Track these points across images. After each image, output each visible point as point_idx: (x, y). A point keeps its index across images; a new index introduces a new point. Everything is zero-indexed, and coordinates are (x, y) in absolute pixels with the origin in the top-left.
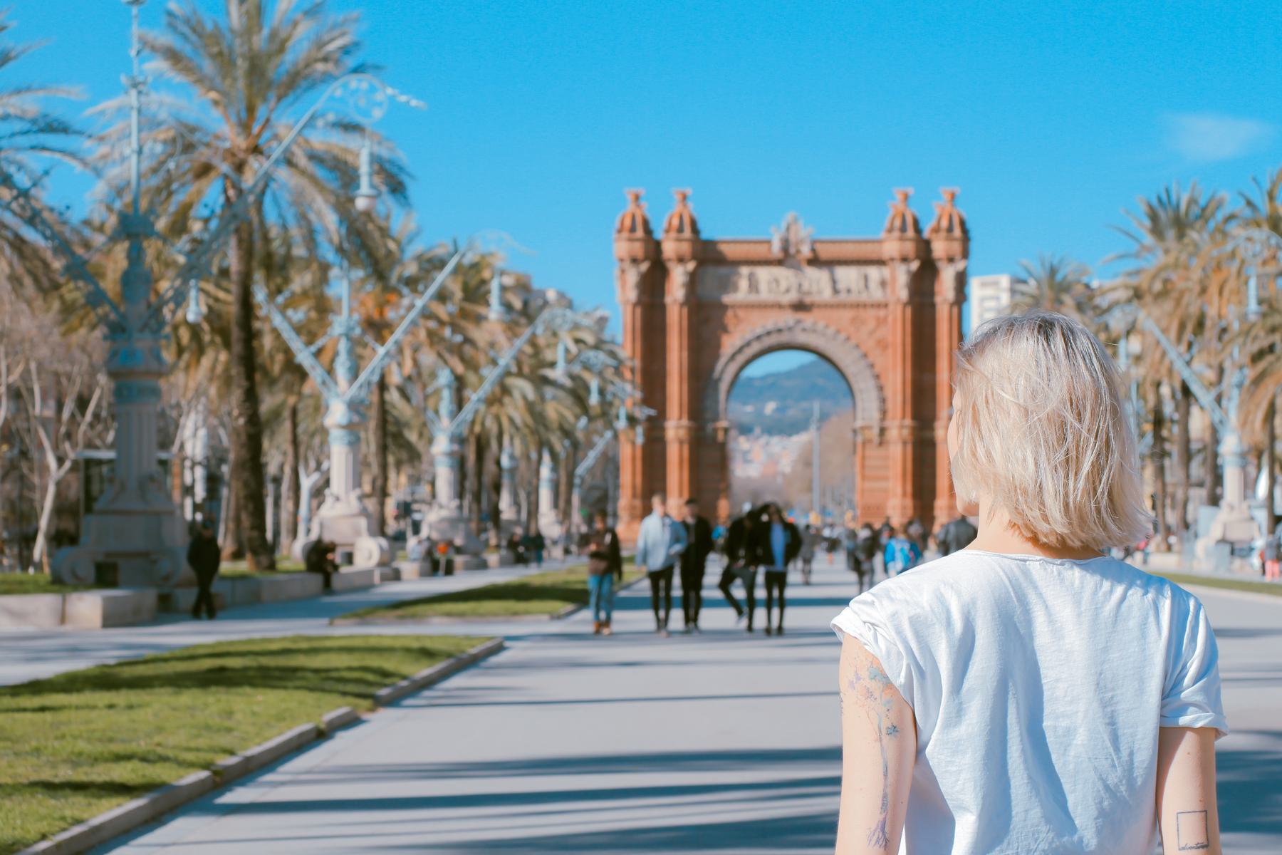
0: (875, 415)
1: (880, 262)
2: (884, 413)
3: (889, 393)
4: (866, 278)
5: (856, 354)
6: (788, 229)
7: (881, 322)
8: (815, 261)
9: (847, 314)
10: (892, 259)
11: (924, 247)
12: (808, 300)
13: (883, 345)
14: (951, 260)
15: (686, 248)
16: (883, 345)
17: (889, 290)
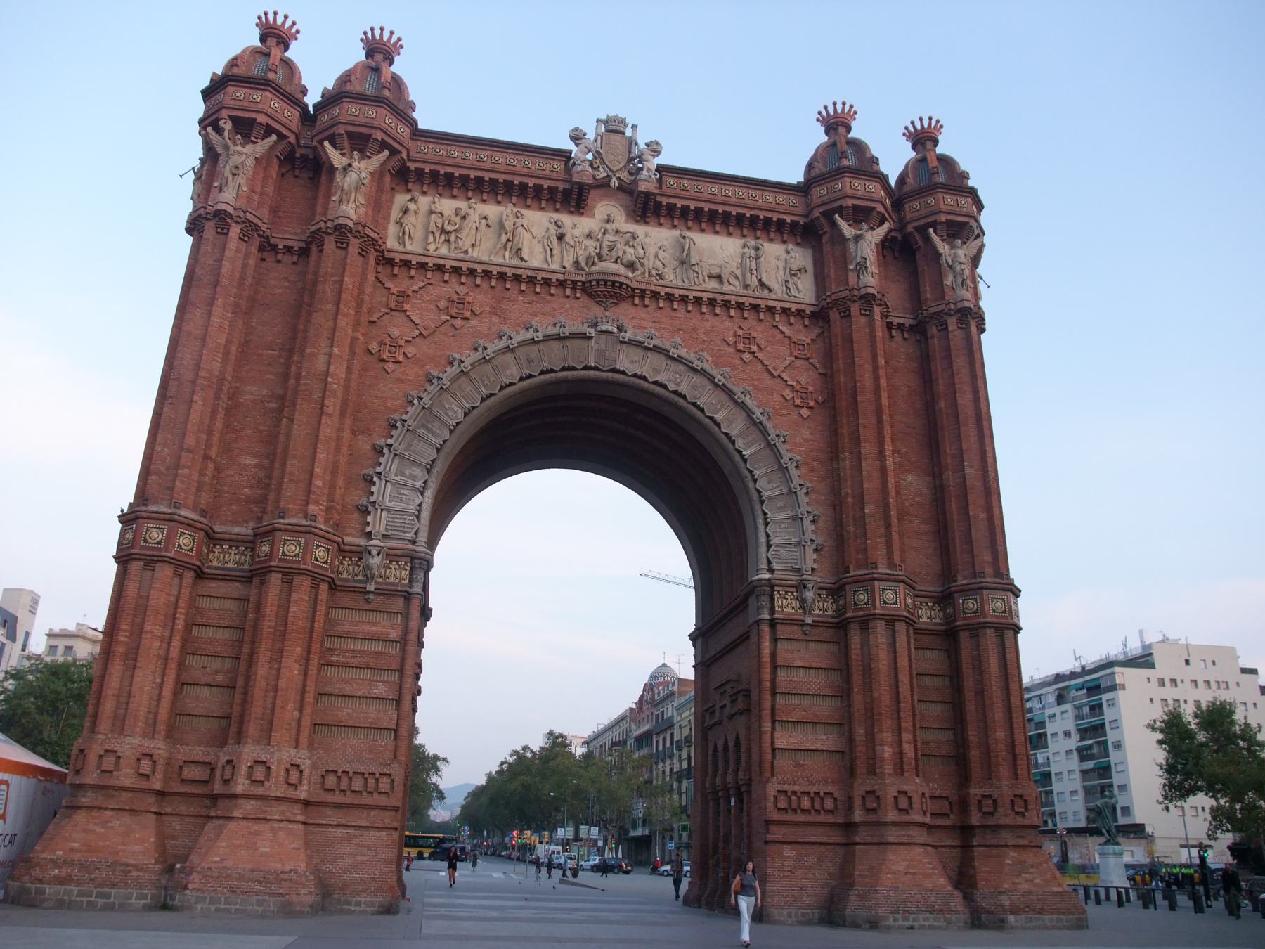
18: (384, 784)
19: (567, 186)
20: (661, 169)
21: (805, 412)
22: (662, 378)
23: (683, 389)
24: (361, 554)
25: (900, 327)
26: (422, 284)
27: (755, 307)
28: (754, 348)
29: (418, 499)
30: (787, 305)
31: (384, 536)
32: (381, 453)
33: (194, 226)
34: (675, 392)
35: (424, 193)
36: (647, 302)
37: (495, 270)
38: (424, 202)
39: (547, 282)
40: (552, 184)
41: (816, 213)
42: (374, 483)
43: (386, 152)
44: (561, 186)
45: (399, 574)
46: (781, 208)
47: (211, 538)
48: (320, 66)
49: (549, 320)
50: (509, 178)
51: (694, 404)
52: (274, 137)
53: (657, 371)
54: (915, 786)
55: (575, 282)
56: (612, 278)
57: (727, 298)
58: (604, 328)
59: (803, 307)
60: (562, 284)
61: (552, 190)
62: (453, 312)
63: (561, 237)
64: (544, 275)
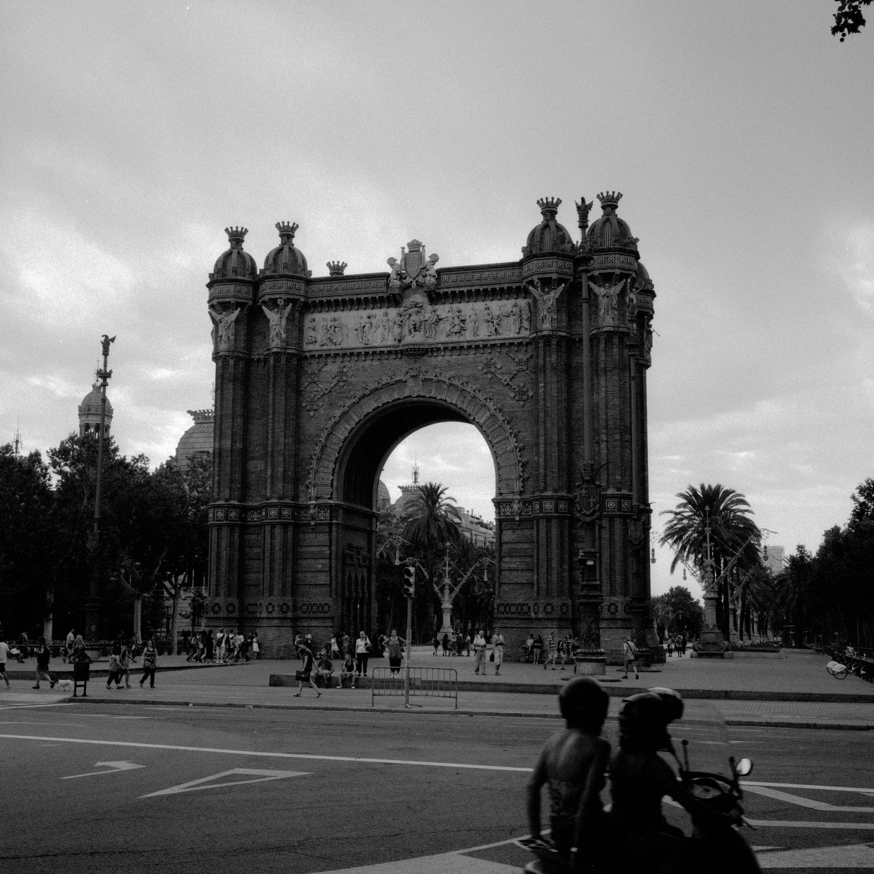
0: (517, 486)
6: (405, 258)
14: (607, 278)
18: (326, 608)
20: (440, 272)
21: (522, 403)
22: (443, 397)
24: (307, 507)
28: (493, 370)
29: (331, 477)
31: (317, 498)
32: (312, 459)
33: (215, 359)
39: (382, 353)
40: (381, 295)
43: (291, 304)
45: (324, 516)
47: (245, 510)
48: (260, 249)
54: (556, 602)
57: (476, 344)
60: (390, 352)
61: (381, 298)
62: (337, 378)
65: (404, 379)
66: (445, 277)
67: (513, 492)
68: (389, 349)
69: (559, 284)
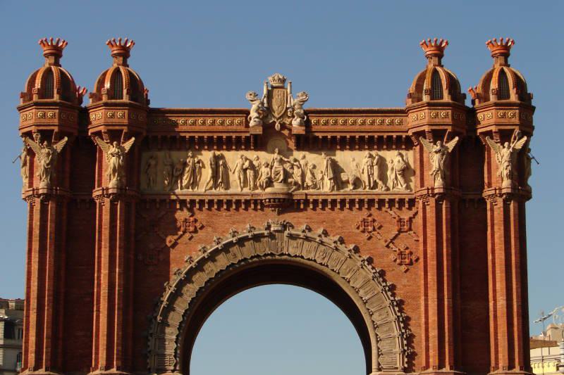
1: (403, 143)
2: (411, 357)
3: (417, 329)
4: (382, 164)
5: (369, 272)
6: (270, 95)
7: (404, 227)
8: (308, 142)
9: (358, 215)
10: (422, 134)
11: (465, 118)
12: (299, 195)
13: (407, 260)
14: (505, 136)
15: (121, 116)
16: (407, 260)
17: (414, 182)
19: (248, 135)
20: (306, 113)
21: (403, 268)
22: (311, 256)
23: (324, 262)
25: (472, 200)
26: (163, 213)
27: (371, 202)
30: (392, 197)
34: (321, 264)
35: (160, 150)
36: (302, 206)
37: (207, 199)
38: (161, 154)
39: (238, 203)
41: (410, 133)
42: (149, 340)
43: (133, 139)
44: (243, 135)
46: (390, 128)
48: (87, 70)
49: (242, 226)
50: (210, 135)
51: (333, 270)
52: (66, 139)
53: (309, 252)
55: (256, 201)
56: (278, 197)
58: (276, 229)
59: (403, 197)
60: (247, 203)
63: (245, 170)
64: (237, 198)
65: (266, 233)
66: (313, 121)
67: (397, 368)
68: (248, 198)
69: (453, 138)
